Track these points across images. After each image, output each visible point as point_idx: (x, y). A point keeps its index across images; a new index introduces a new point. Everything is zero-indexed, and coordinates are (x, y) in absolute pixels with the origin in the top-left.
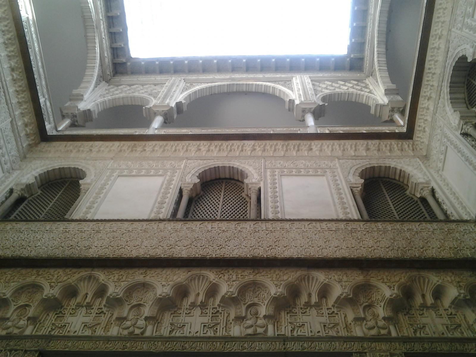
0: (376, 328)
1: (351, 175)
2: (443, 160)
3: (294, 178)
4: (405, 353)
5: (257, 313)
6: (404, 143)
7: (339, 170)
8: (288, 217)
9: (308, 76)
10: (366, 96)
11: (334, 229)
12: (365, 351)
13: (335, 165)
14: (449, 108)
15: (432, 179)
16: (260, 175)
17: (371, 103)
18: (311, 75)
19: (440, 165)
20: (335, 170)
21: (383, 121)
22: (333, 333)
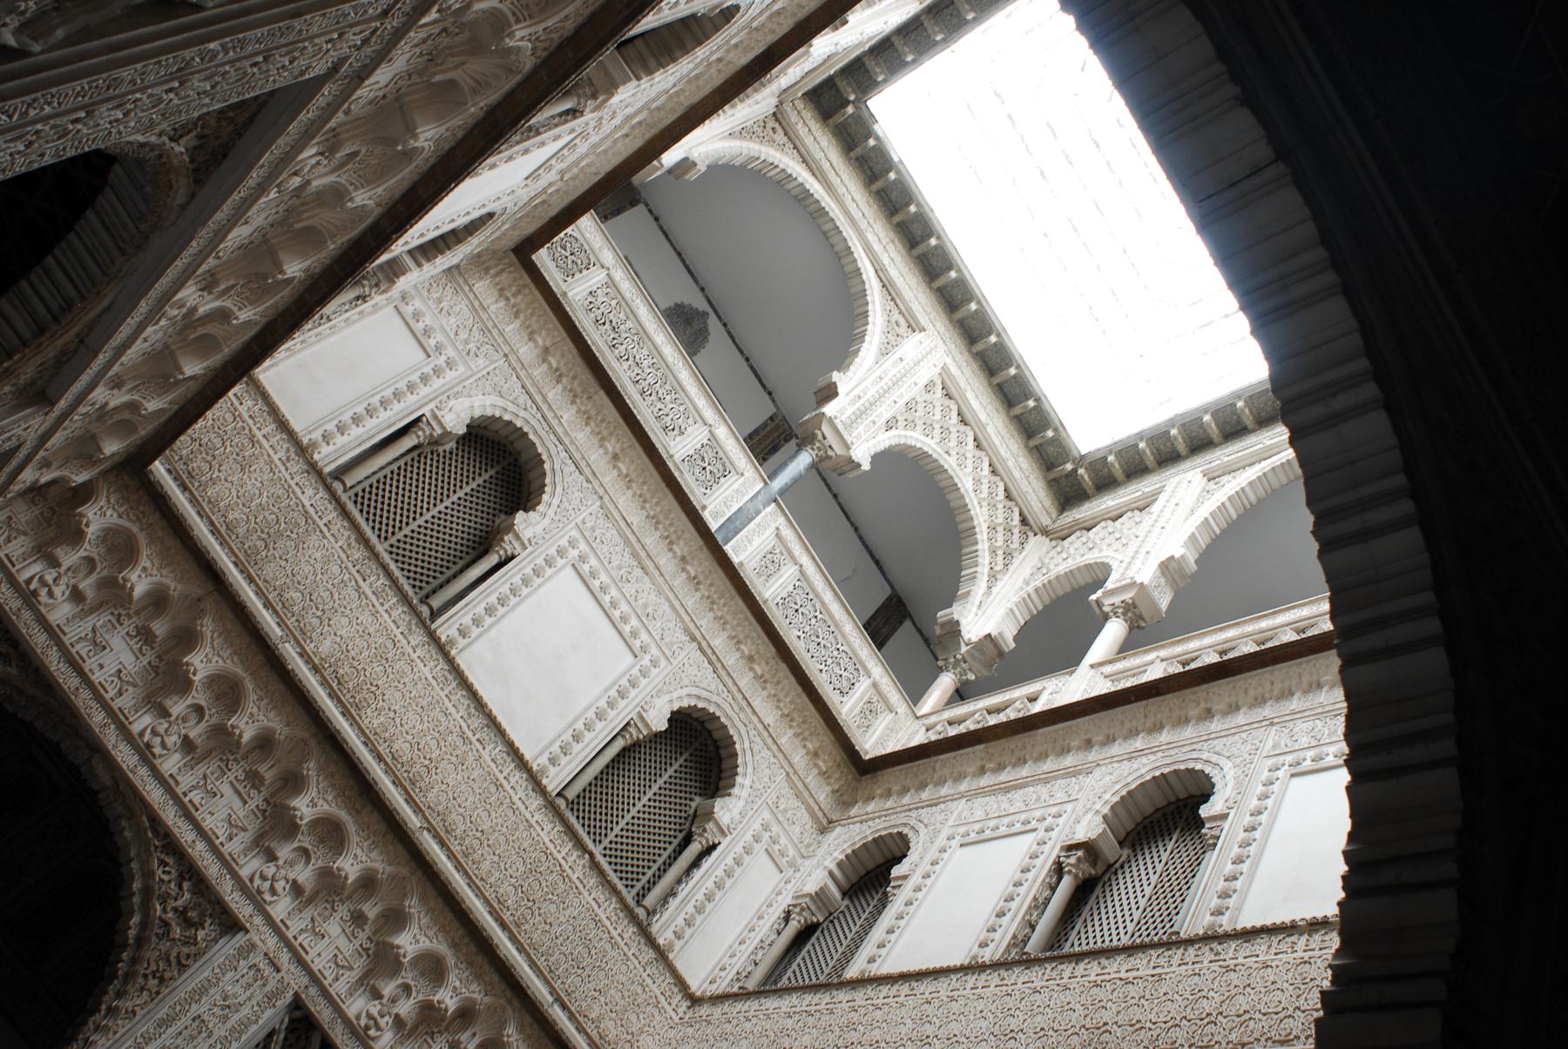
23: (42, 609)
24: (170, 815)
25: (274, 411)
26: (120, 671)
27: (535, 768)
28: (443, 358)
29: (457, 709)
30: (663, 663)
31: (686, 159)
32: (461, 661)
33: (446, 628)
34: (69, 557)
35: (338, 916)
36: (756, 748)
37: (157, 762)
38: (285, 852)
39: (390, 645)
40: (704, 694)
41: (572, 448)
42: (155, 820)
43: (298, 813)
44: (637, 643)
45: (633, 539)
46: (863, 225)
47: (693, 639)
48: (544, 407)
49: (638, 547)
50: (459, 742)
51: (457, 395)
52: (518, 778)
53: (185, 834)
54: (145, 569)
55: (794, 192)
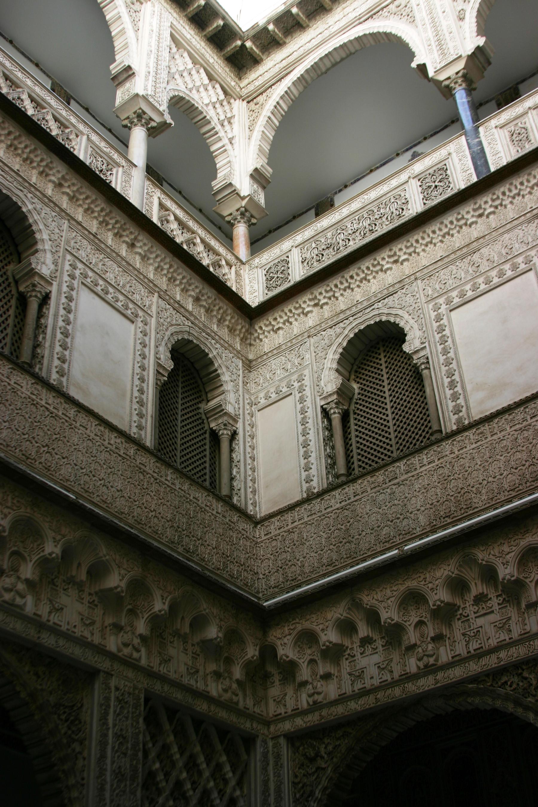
0: (131, 646)
1: (163, 343)
2: (271, 401)
3: (97, 299)
4: (146, 689)
6: (240, 321)
7: (153, 321)
9: (171, 19)
10: (224, 146)
11: (121, 453)
12: (113, 673)
13: (150, 307)
14: (332, 357)
15: (241, 417)
16: (55, 263)
17: (220, 162)
18: (175, 23)
19: (263, 401)
21: (218, 211)
22: (87, 634)
23: (325, 702)
24: (474, 668)
25: (281, 512)
26: (379, 667)
28: (296, 385)
29: (505, 428)
31: (251, 175)
32: (476, 416)
33: (450, 423)
34: (304, 673)
37: (440, 663)
39: (441, 471)
41: (380, 296)
42: (475, 679)
43: (508, 577)
44: (523, 266)
45: (453, 256)
46: (326, 34)
48: (348, 313)
49: (459, 253)
50: (526, 434)
51: (319, 379)
53: (491, 662)
54: (323, 630)
55: (301, 88)
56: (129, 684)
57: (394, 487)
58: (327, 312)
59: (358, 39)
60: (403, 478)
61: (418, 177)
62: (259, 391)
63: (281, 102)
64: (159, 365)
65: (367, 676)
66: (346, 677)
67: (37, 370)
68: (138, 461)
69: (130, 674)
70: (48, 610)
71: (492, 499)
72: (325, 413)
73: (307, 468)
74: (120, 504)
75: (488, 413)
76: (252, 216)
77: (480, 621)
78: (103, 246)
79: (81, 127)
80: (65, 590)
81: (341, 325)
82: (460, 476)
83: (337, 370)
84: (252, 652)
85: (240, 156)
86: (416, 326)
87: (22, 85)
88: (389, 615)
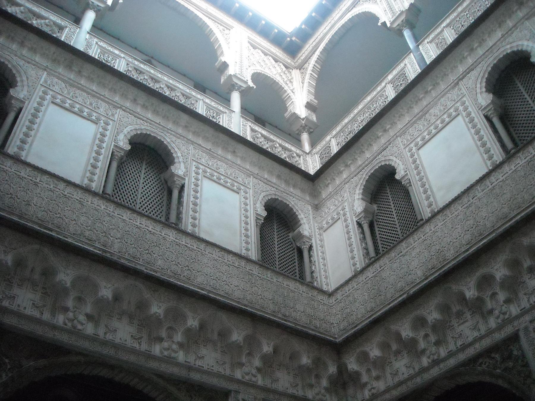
0: (250, 374)
1: (259, 202)
2: (329, 225)
4: (263, 399)
5: (172, 338)
7: (251, 191)
8: (203, 236)
13: (249, 183)
14: (358, 193)
16: (186, 168)
20: (248, 190)
24: (462, 357)
26: (406, 366)
27: (491, 168)
28: (341, 212)
29: (458, 208)
30: (464, 99)
31: (306, 106)
32: (441, 204)
34: (365, 378)
35: (528, 281)
36: (511, 40)
37: (441, 358)
38: (489, 305)
39: (426, 242)
40: (481, 74)
41: (379, 151)
43: (472, 297)
44: (454, 114)
46: (333, 22)
47: (457, 84)
48: (364, 165)
50: (471, 209)
52: (493, 178)
53: (471, 352)
54: (371, 350)
56: (251, 397)
57: (401, 258)
58: (353, 168)
59: (350, 20)
60: (405, 251)
61: (390, 82)
62: (323, 221)
63: (316, 64)
64: (257, 214)
65: (400, 374)
66: (389, 376)
67: (180, 226)
68: (248, 268)
69: (252, 391)
70: (194, 358)
71: (457, 252)
72: (359, 225)
73: (353, 258)
74: (238, 294)
75: (447, 202)
76: (310, 128)
77: (462, 327)
78: (215, 155)
79: (199, 96)
80: (204, 346)
81: (361, 173)
82: (437, 243)
83: (362, 199)
84: (332, 369)
85: (299, 98)
86: (401, 163)
87: (161, 80)
88: (406, 333)
